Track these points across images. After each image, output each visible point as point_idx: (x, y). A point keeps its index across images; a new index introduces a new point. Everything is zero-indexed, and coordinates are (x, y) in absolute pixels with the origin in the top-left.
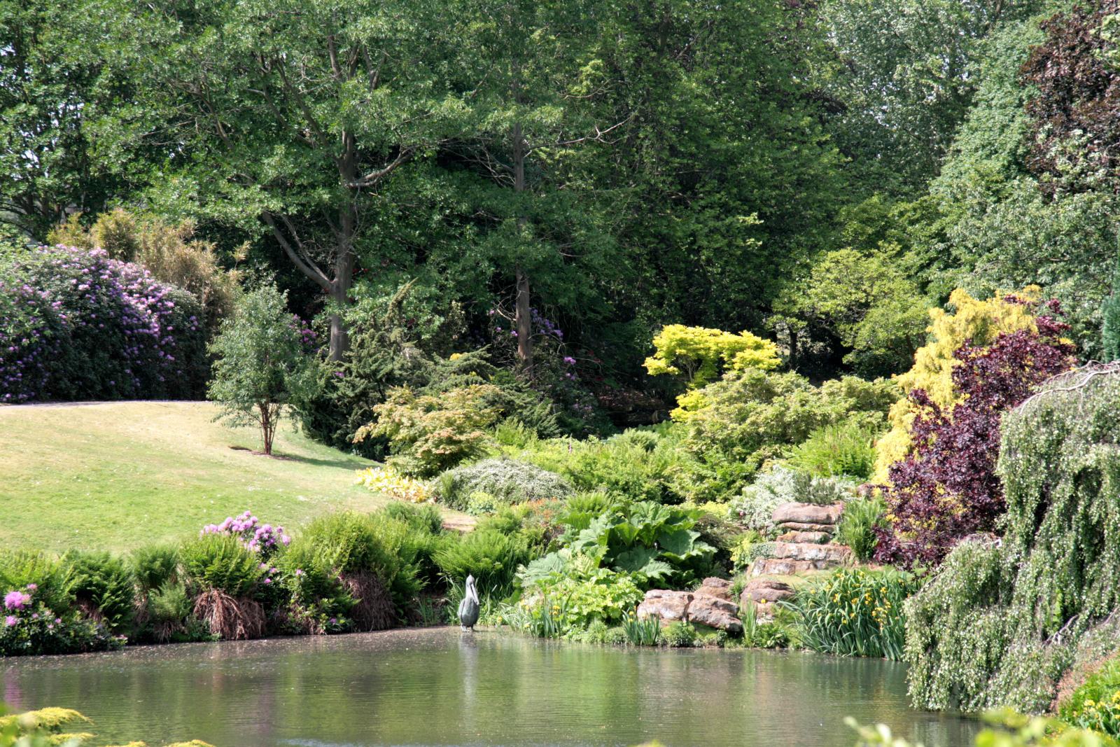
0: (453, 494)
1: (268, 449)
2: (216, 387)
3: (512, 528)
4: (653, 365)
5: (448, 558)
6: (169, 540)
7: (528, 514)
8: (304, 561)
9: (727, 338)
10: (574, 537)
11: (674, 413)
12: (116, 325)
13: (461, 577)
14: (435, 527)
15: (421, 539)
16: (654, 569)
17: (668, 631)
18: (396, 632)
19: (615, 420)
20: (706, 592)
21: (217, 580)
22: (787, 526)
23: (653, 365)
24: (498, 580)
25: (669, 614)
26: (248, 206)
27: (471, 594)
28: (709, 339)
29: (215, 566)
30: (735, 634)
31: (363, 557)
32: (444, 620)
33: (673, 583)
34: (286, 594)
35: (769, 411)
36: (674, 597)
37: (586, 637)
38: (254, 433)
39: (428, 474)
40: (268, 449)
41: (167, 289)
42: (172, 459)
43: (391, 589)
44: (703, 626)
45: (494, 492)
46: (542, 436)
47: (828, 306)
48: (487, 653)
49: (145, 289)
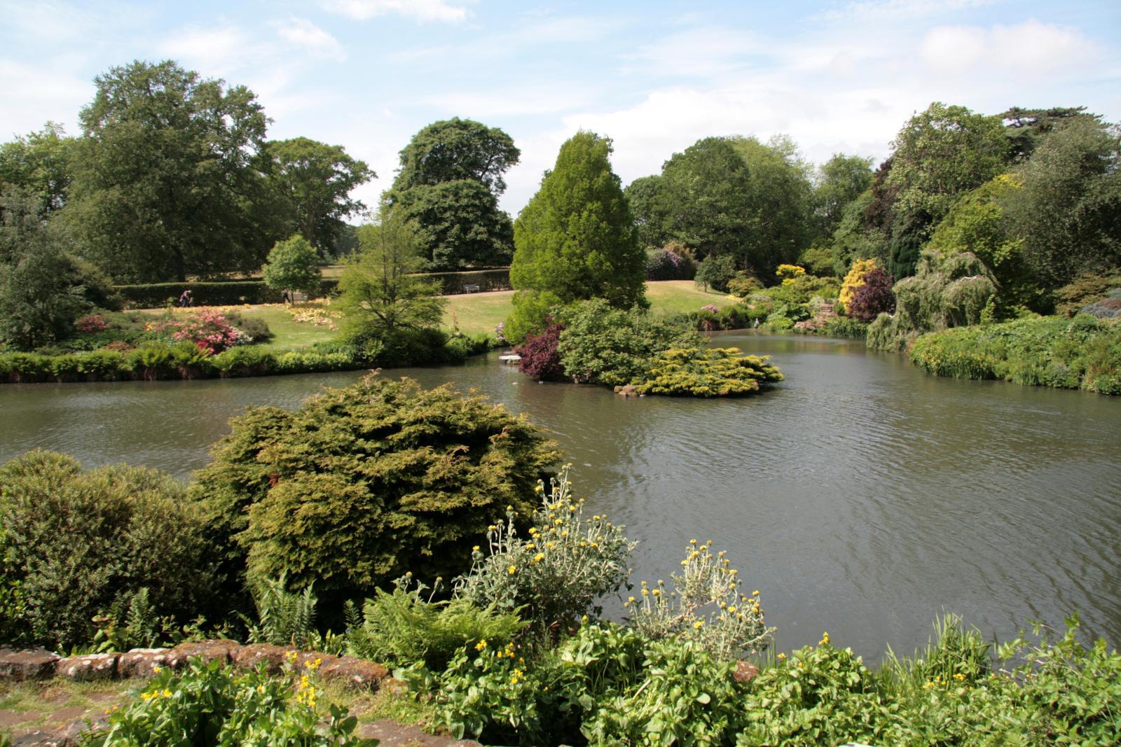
0: (748, 301)
3: (763, 308)
4: (778, 273)
5: (750, 315)
6: (695, 310)
8: (723, 314)
9: (794, 267)
13: (754, 319)
14: (746, 308)
15: (744, 311)
17: (801, 330)
19: (768, 286)
20: (808, 323)
21: (706, 319)
22: (823, 309)
24: (763, 319)
26: (697, 241)
27: (757, 322)
28: (790, 267)
30: (816, 331)
31: (734, 314)
32: (749, 327)
33: (799, 320)
36: (803, 323)
38: (703, 288)
39: (741, 297)
42: (689, 293)
43: (739, 321)
44: (809, 329)
47: (808, 261)
49: (676, 259)
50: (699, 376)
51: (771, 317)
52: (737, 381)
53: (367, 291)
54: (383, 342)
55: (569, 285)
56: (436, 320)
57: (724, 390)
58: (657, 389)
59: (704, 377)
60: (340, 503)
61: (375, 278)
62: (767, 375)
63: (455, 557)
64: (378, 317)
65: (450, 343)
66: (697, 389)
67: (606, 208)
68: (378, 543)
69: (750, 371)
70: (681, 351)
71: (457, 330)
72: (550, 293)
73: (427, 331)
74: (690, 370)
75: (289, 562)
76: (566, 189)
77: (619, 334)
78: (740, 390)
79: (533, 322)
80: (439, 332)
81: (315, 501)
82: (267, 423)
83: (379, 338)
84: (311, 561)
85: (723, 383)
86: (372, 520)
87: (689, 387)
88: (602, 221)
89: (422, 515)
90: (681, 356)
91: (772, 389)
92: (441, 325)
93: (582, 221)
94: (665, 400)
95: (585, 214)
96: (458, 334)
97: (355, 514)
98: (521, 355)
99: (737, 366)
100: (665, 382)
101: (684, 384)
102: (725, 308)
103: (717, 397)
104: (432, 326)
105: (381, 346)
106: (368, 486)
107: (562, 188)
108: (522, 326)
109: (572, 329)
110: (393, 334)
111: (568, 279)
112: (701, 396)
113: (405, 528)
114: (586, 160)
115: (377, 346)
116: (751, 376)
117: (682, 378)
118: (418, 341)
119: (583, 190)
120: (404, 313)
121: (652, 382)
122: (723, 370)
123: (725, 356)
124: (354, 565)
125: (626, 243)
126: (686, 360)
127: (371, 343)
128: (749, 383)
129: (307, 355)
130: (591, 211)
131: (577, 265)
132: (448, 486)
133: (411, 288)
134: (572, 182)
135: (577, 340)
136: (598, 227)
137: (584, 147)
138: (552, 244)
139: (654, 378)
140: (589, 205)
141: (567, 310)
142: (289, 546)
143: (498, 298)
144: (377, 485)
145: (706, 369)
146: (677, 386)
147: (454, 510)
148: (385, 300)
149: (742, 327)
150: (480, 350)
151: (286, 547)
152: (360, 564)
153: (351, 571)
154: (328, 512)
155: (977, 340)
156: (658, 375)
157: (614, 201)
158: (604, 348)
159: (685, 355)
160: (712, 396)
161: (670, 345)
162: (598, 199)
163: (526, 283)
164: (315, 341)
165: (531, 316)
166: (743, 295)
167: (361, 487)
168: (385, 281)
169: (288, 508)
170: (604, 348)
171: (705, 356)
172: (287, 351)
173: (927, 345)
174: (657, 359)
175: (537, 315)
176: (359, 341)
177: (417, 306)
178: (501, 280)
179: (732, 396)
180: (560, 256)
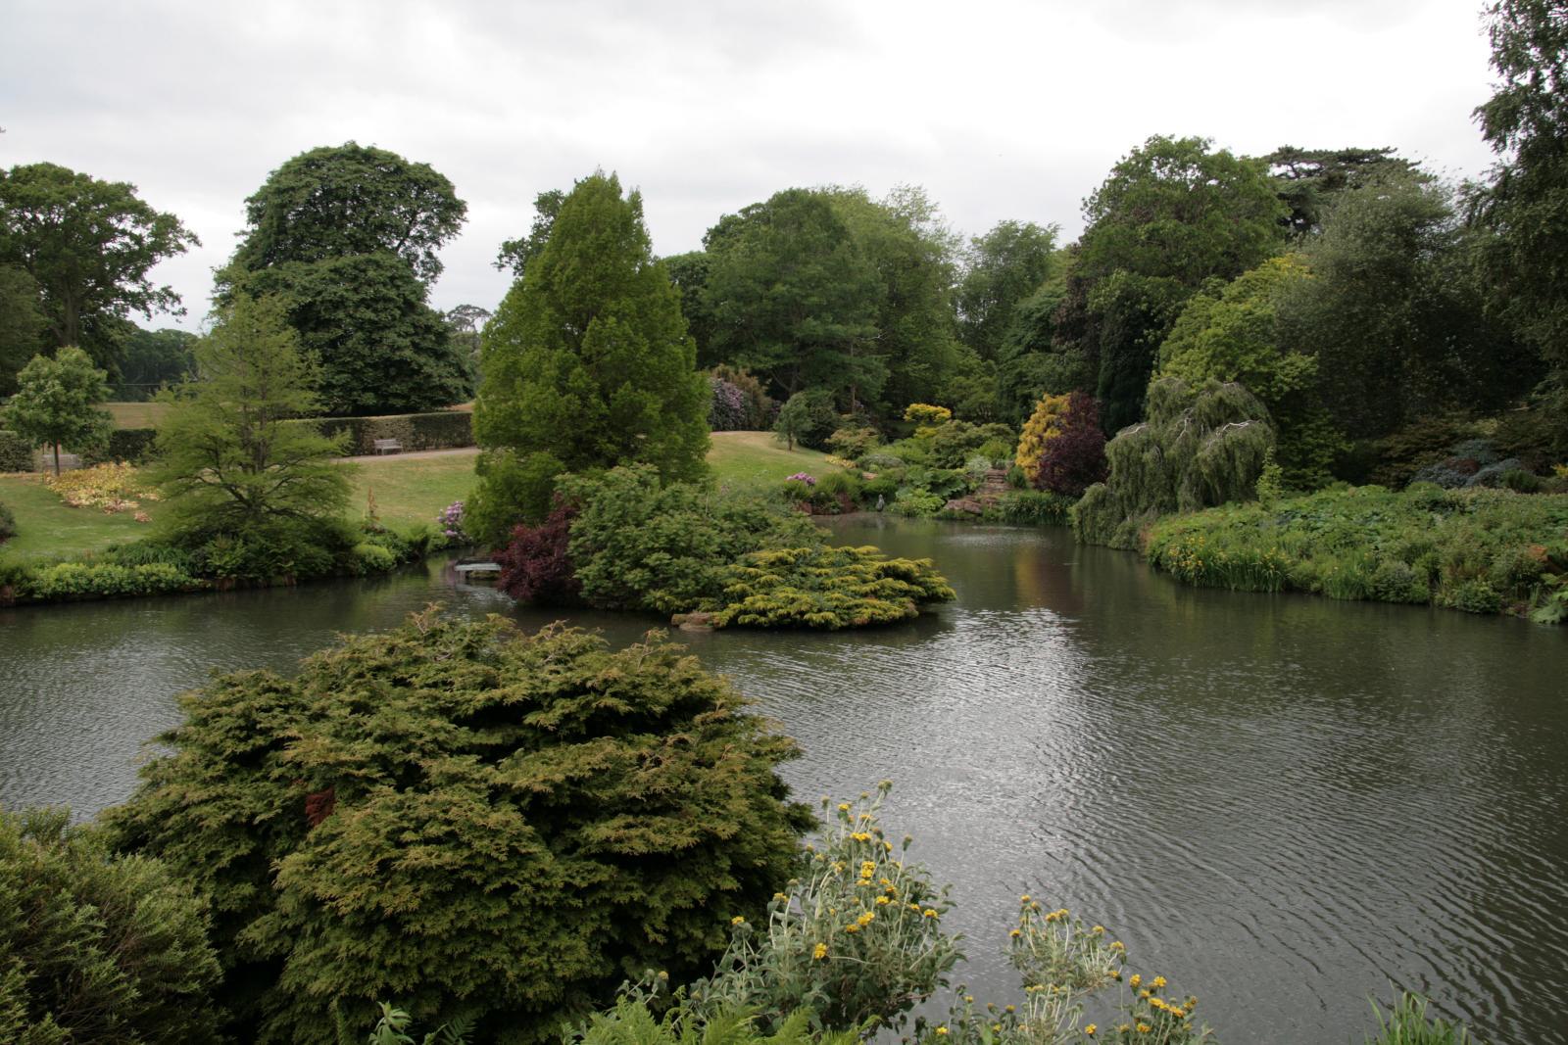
9: (932, 409)
14: (860, 476)
15: (857, 482)
16: (947, 493)
17: (957, 514)
22: (989, 477)
27: (881, 501)
31: (841, 489)
35: (964, 436)
38: (786, 444)
39: (850, 458)
52: (886, 604)
53: (213, 452)
54: (245, 543)
56: (339, 503)
57: (864, 615)
58: (747, 619)
60: (486, 842)
61: (230, 427)
62: (927, 589)
64: (234, 498)
69: (903, 585)
70: (783, 553)
73: (322, 522)
80: (345, 522)
81: (427, 841)
82: (262, 701)
83: (235, 535)
84: (427, 961)
85: (857, 606)
87: (802, 613)
89: (626, 862)
90: (782, 561)
92: (348, 511)
98: (500, 562)
99: (878, 577)
100: (760, 605)
101: (792, 609)
104: (333, 514)
105: (240, 550)
106: (521, 810)
112: (824, 630)
113: (600, 886)
114: (590, 226)
115: (233, 549)
116: (906, 593)
121: (737, 606)
123: (856, 560)
127: (223, 542)
128: (902, 605)
129: (98, 568)
133: (296, 443)
135: (603, 535)
138: (550, 371)
142: (380, 936)
145: (828, 582)
146: (781, 611)
148: (245, 467)
150: (415, 555)
151: (375, 938)
155: (1271, 527)
164: (109, 541)
168: (243, 431)
171: (823, 560)
172: (57, 562)
173: (1185, 533)
176: (194, 540)
178: (454, 433)
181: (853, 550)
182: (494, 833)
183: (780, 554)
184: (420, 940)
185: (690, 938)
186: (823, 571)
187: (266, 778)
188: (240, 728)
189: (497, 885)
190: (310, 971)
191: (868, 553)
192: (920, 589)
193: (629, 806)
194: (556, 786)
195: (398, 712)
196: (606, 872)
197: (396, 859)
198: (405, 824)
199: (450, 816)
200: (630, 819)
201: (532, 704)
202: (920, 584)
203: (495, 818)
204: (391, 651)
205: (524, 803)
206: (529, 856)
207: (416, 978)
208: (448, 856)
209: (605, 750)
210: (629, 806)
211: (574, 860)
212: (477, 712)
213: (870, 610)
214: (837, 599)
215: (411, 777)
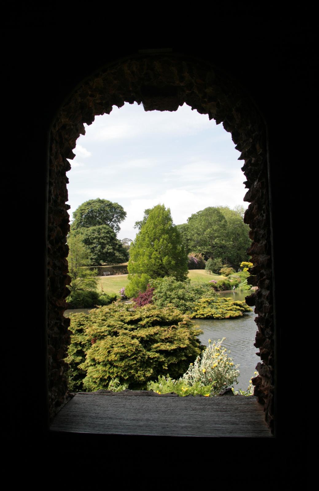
0: (230, 278)
1: (210, 274)
2: (205, 268)
3: (236, 281)
5: (231, 284)
7: (238, 280)
8: (219, 284)
9: (248, 263)
10: (243, 282)
11: (243, 270)
12: (193, 263)
13: (233, 286)
14: (229, 281)
15: (228, 282)
18: (227, 291)
23: (241, 266)
24: (237, 286)
25: (254, 289)
27: (234, 287)
29: (212, 285)
31: (224, 284)
32: (231, 290)
34: (217, 287)
37: (246, 291)
38: (209, 273)
39: (226, 276)
40: (210, 274)
41: (197, 259)
42: (203, 275)
45: (233, 278)
46: (235, 272)
48: (236, 293)
49: (196, 260)
50: (216, 310)
51: (240, 285)
52: (234, 312)
54: (72, 297)
55: (154, 271)
56: (94, 287)
57: (227, 316)
58: (198, 316)
59: (218, 310)
60: (131, 347)
62: (245, 309)
63: (173, 370)
65: (100, 298)
66: (216, 316)
67: (170, 237)
68: (146, 363)
69: (238, 307)
70: (207, 299)
71: (103, 291)
72: (146, 275)
73: (90, 292)
74: (212, 308)
75: (109, 372)
76: (154, 229)
77: (180, 292)
78: (234, 316)
79: (138, 287)
80: (96, 292)
82: (82, 319)
85: (226, 313)
86: (143, 354)
87: (212, 315)
88: (169, 243)
89: (161, 352)
90: (207, 301)
91: (247, 315)
92: (96, 289)
93: (160, 243)
94: (202, 320)
95: (161, 240)
96: (103, 293)
97: (138, 351)
99: (232, 305)
100: (202, 313)
101: (210, 314)
102: (220, 281)
103: (225, 319)
104: (93, 290)
107: (151, 228)
108: (134, 290)
109: (159, 290)
110: (76, 293)
111: (155, 268)
112: (218, 319)
113: (156, 357)
116: (239, 310)
117: (208, 311)
118: (87, 297)
119: (160, 229)
120: (81, 284)
121: (196, 313)
122: (226, 307)
123: (226, 301)
124: (137, 373)
125: (179, 253)
126: (210, 303)
128: (238, 313)
130: (164, 239)
131: (159, 262)
132: (170, 340)
133: (84, 273)
134: (156, 226)
135: (161, 295)
136: (167, 246)
137: (161, 211)
138: (147, 253)
139: (196, 311)
140: (163, 236)
141: (155, 281)
142: (108, 366)
143: (119, 278)
144: (142, 340)
145: (219, 307)
147: (174, 350)
149: (227, 289)
151: (107, 367)
152: (139, 372)
153: (136, 375)
154: (126, 351)
156: (198, 309)
157: (174, 234)
158: (174, 298)
159: (209, 301)
160: (222, 319)
161: (202, 297)
162: (167, 233)
163: (134, 271)
165: (138, 285)
166: (227, 275)
167: (136, 341)
169: (108, 350)
170: (174, 298)
171: (218, 301)
174: (197, 303)
175: (140, 284)
177: (86, 281)
178: (124, 270)
179: (231, 318)
180: (150, 258)
181: (225, 298)
182: (132, 345)
183: (206, 300)
184: (117, 367)
185: (175, 371)
186: (218, 304)
187: (83, 335)
188: (78, 324)
189: (134, 357)
190: (93, 373)
191: (230, 299)
192: (243, 309)
193: (163, 341)
194: (147, 336)
195: (111, 321)
196: (157, 355)
197: (111, 350)
198: (113, 343)
199: (123, 342)
200: (162, 343)
201: (140, 319)
202: (243, 307)
203: (133, 342)
204: (110, 309)
205: (139, 339)
206: (140, 351)
207: (116, 375)
208: (123, 350)
209: (157, 329)
210: (163, 341)
211: (150, 352)
212: (128, 321)
213: (230, 314)
214: (221, 311)
215: (116, 334)
